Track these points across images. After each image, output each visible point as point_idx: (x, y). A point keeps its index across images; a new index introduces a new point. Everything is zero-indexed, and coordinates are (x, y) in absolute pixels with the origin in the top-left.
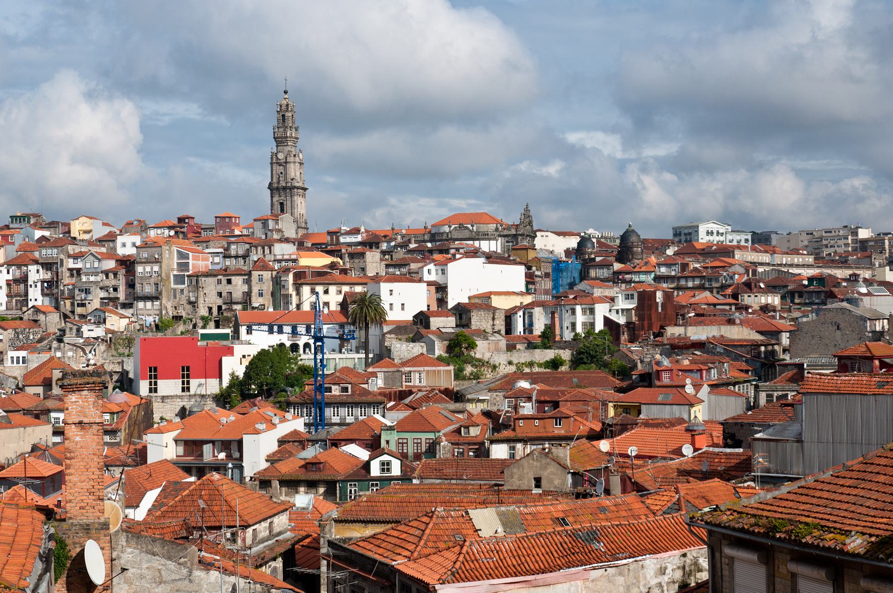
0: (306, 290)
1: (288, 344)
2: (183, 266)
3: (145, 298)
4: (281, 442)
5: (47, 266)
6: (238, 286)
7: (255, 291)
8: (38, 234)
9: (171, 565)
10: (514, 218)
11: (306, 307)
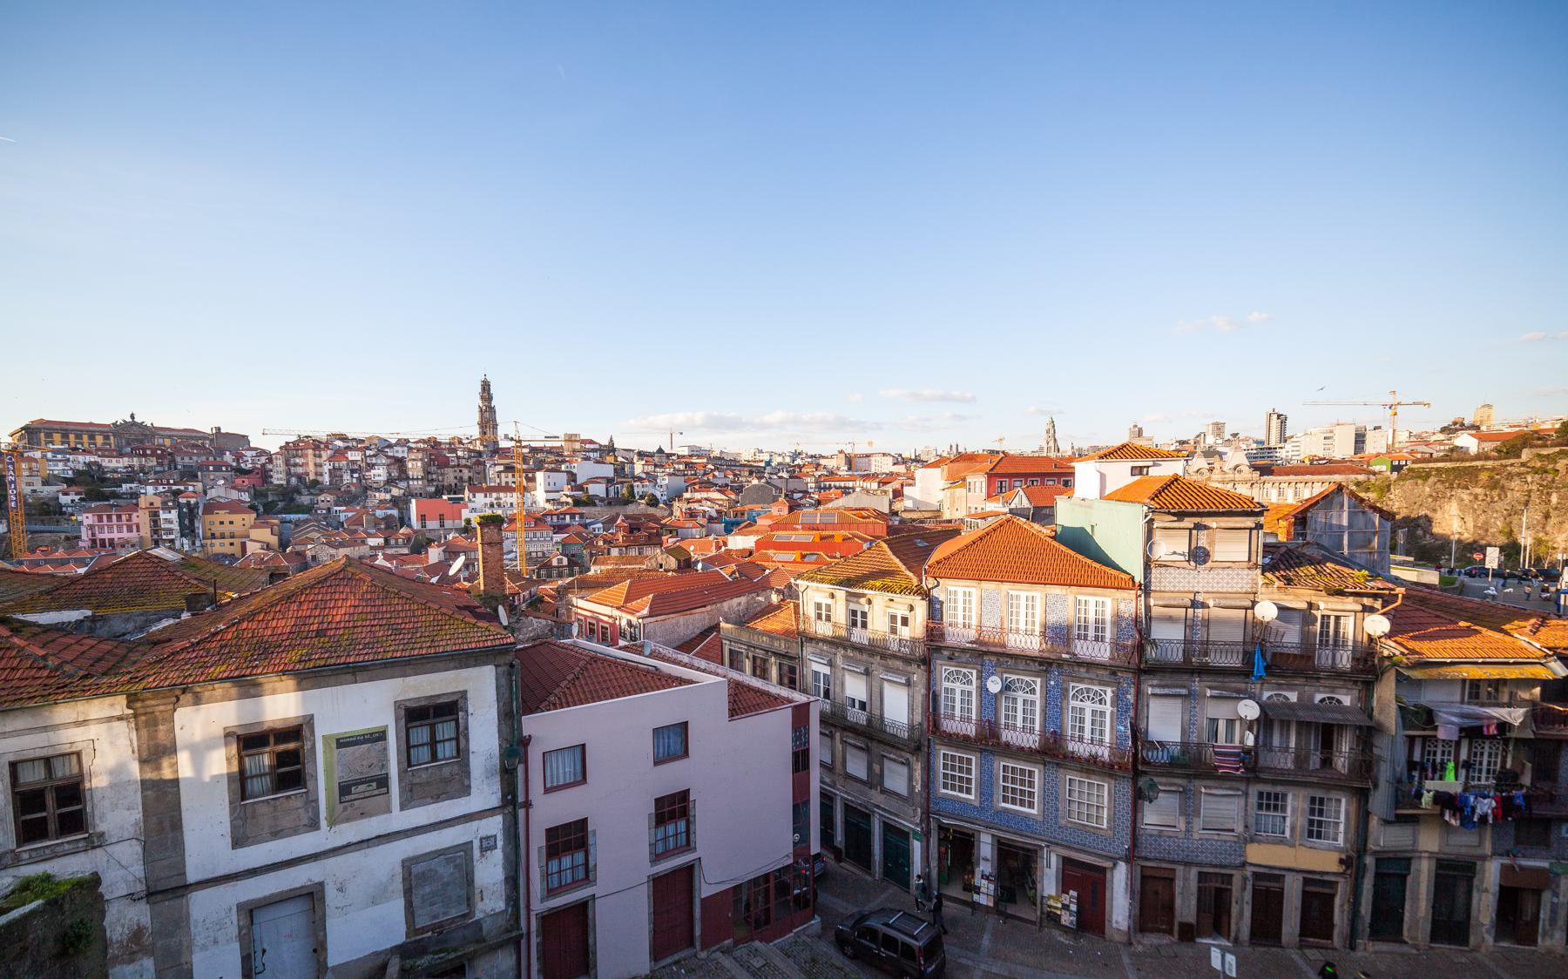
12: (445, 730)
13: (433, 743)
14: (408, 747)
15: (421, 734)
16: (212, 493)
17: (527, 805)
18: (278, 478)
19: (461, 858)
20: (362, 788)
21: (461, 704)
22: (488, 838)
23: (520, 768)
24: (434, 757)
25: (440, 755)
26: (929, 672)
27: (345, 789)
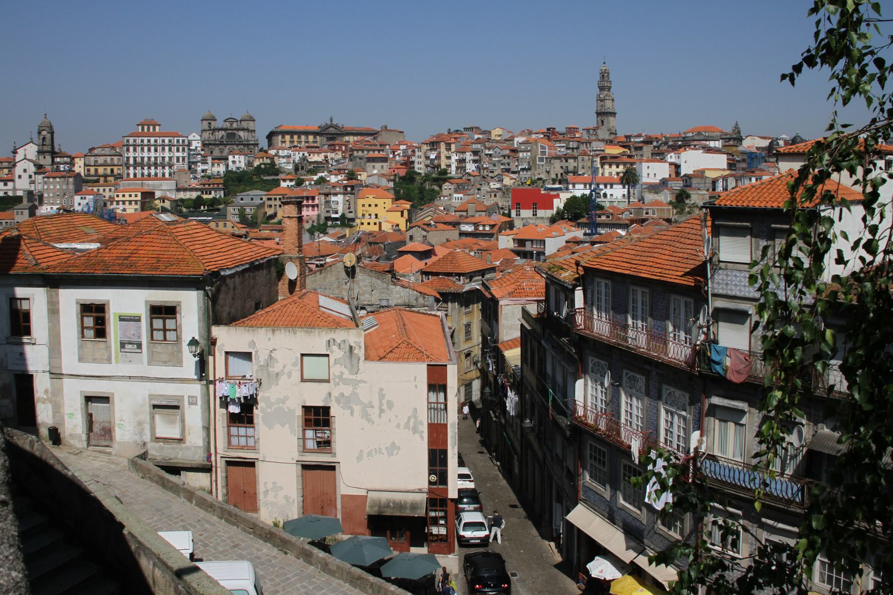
2: (543, 153)
4: (567, 242)
5: (475, 153)
7: (580, 166)
8: (476, 137)
9: (379, 282)
11: (607, 175)
12: (170, 324)
13: (165, 330)
15: (158, 323)
16: (370, 181)
18: (420, 167)
20: (130, 346)
21: (178, 309)
23: (211, 358)
24: (165, 339)
25: (168, 338)
27: (123, 345)
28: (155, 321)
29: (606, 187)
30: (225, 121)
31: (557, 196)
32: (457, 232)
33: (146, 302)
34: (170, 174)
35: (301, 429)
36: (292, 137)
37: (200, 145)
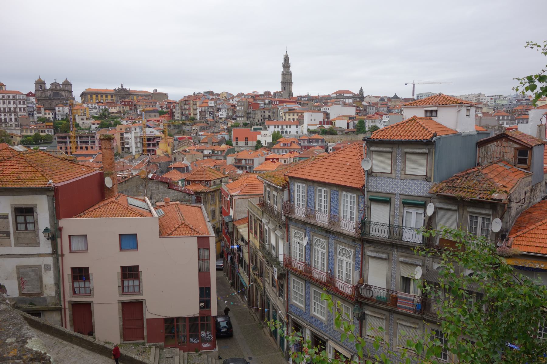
0: (287, 115)
1: (280, 131)
3: (239, 117)
6: (267, 114)
8: (211, 97)
10: (357, 92)
11: (287, 120)
12: (29, 219)
13: (26, 223)
14: (17, 223)
15: (21, 219)
17: (63, 255)
18: (177, 116)
19: (36, 269)
22: (47, 265)
23: (59, 240)
24: (26, 229)
26: (288, 231)
28: (18, 218)
29: (287, 127)
30: (52, 84)
31: (260, 133)
32: (202, 155)
33: (12, 206)
34: (15, 119)
35: (120, 281)
36: (97, 96)
37: (34, 100)
